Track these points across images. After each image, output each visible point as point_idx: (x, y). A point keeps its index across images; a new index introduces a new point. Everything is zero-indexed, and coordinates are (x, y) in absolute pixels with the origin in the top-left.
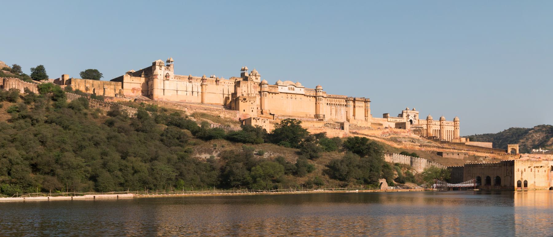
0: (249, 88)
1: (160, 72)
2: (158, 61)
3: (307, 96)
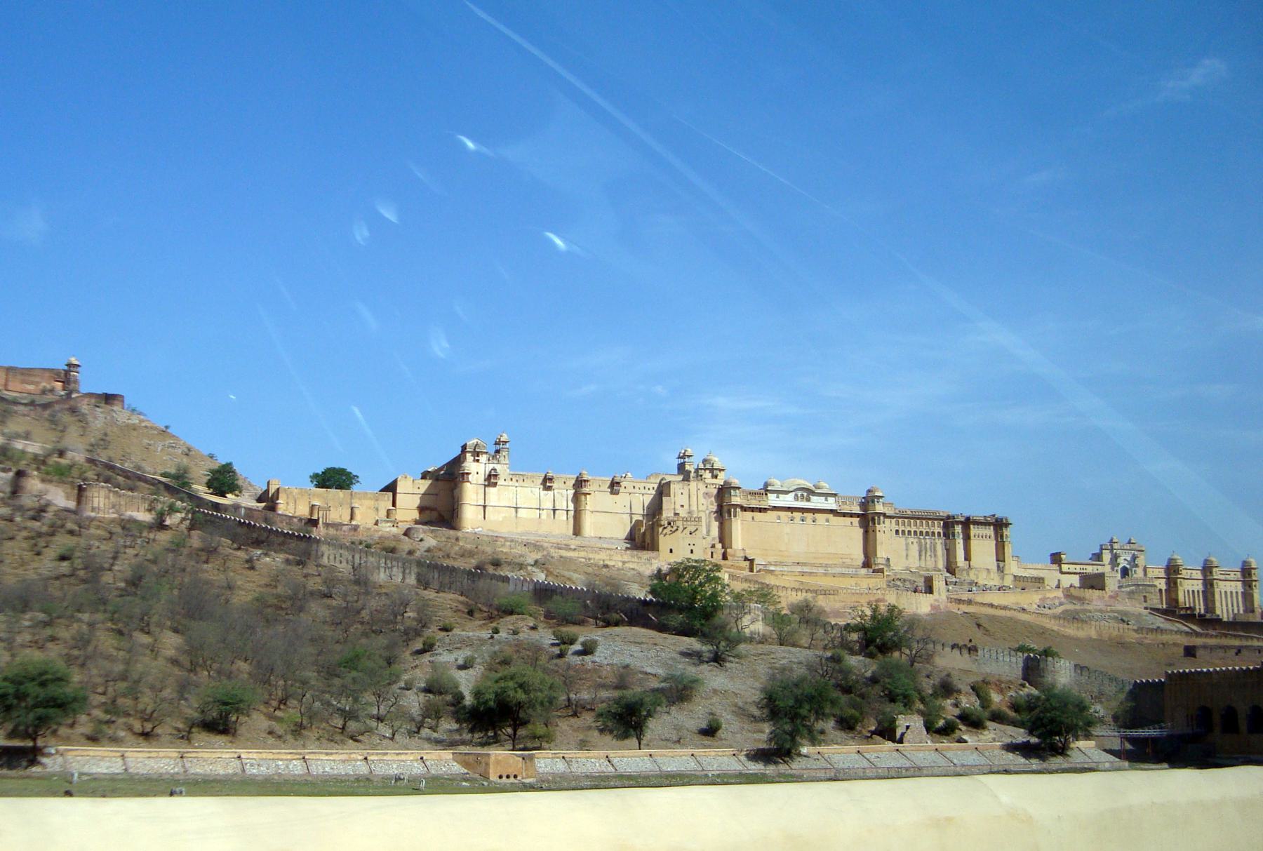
0: (694, 499)
1: (476, 469)
2: (471, 443)
3: (844, 515)
